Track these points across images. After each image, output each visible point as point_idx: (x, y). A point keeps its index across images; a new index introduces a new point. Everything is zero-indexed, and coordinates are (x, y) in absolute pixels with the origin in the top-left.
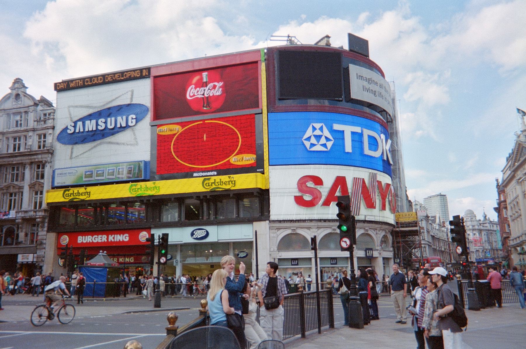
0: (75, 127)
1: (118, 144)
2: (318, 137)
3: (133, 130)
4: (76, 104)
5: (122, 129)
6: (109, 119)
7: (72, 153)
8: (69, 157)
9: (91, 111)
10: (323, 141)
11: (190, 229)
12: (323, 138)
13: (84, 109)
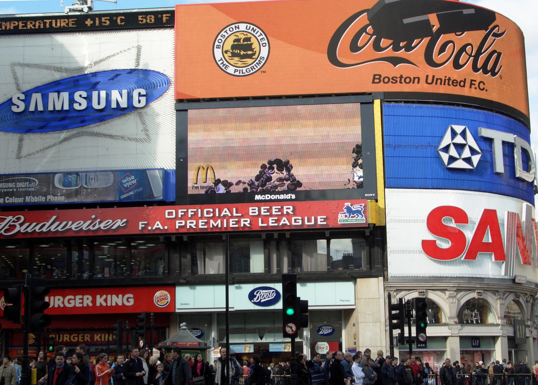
0: (27, 101)
1: (111, 136)
2: (460, 147)
3: (140, 115)
4: (26, 62)
5: (120, 111)
6: (95, 94)
7: (20, 148)
8: (14, 155)
9: (57, 76)
10: (466, 153)
11: (248, 288)
12: (467, 149)
13: (45, 71)
